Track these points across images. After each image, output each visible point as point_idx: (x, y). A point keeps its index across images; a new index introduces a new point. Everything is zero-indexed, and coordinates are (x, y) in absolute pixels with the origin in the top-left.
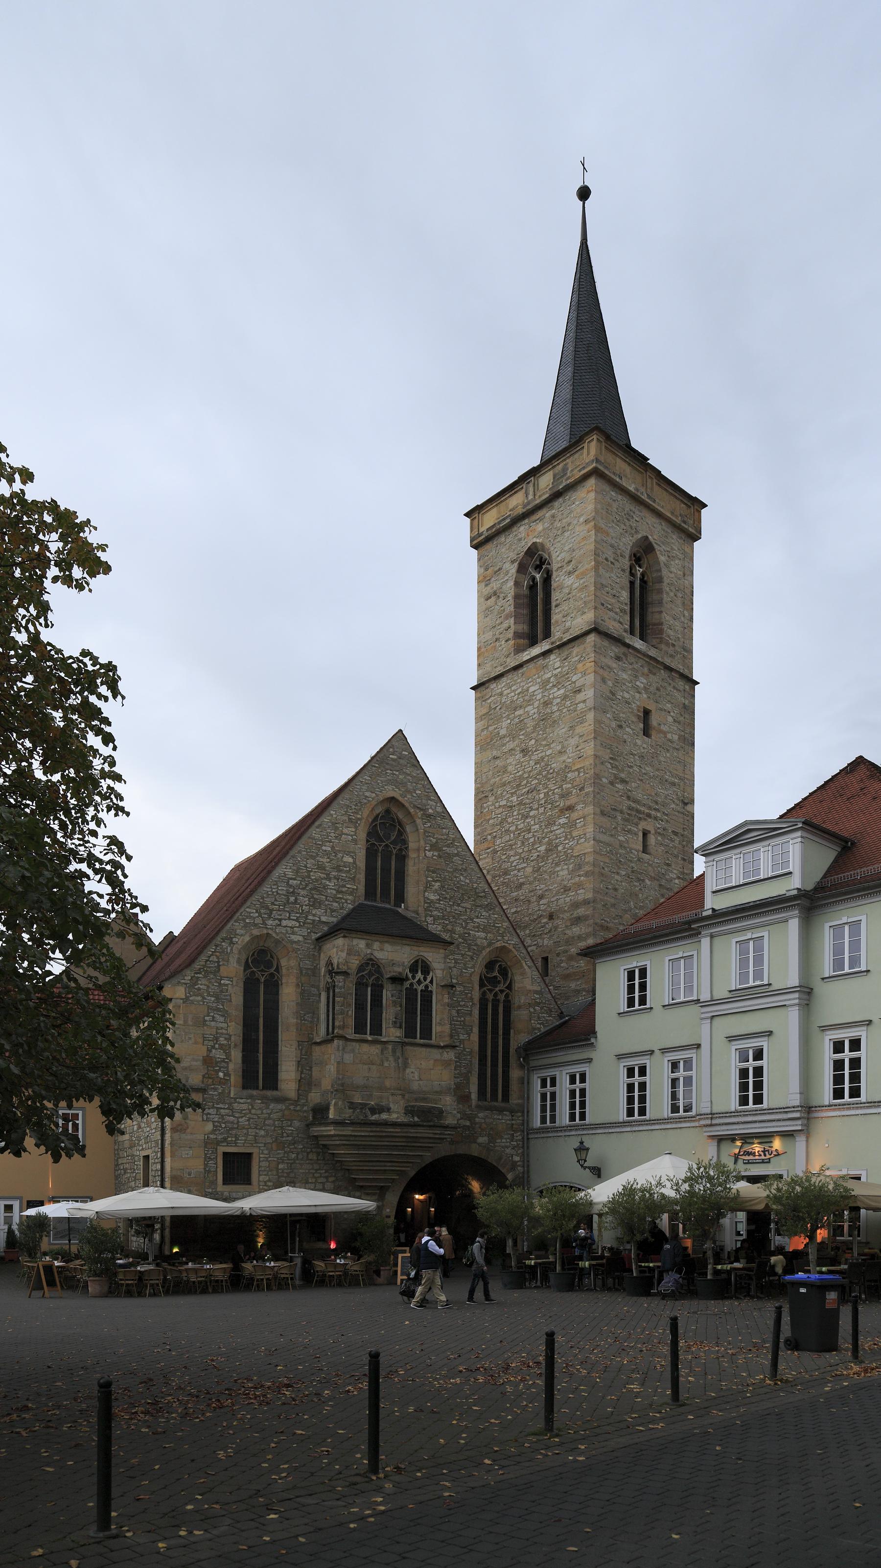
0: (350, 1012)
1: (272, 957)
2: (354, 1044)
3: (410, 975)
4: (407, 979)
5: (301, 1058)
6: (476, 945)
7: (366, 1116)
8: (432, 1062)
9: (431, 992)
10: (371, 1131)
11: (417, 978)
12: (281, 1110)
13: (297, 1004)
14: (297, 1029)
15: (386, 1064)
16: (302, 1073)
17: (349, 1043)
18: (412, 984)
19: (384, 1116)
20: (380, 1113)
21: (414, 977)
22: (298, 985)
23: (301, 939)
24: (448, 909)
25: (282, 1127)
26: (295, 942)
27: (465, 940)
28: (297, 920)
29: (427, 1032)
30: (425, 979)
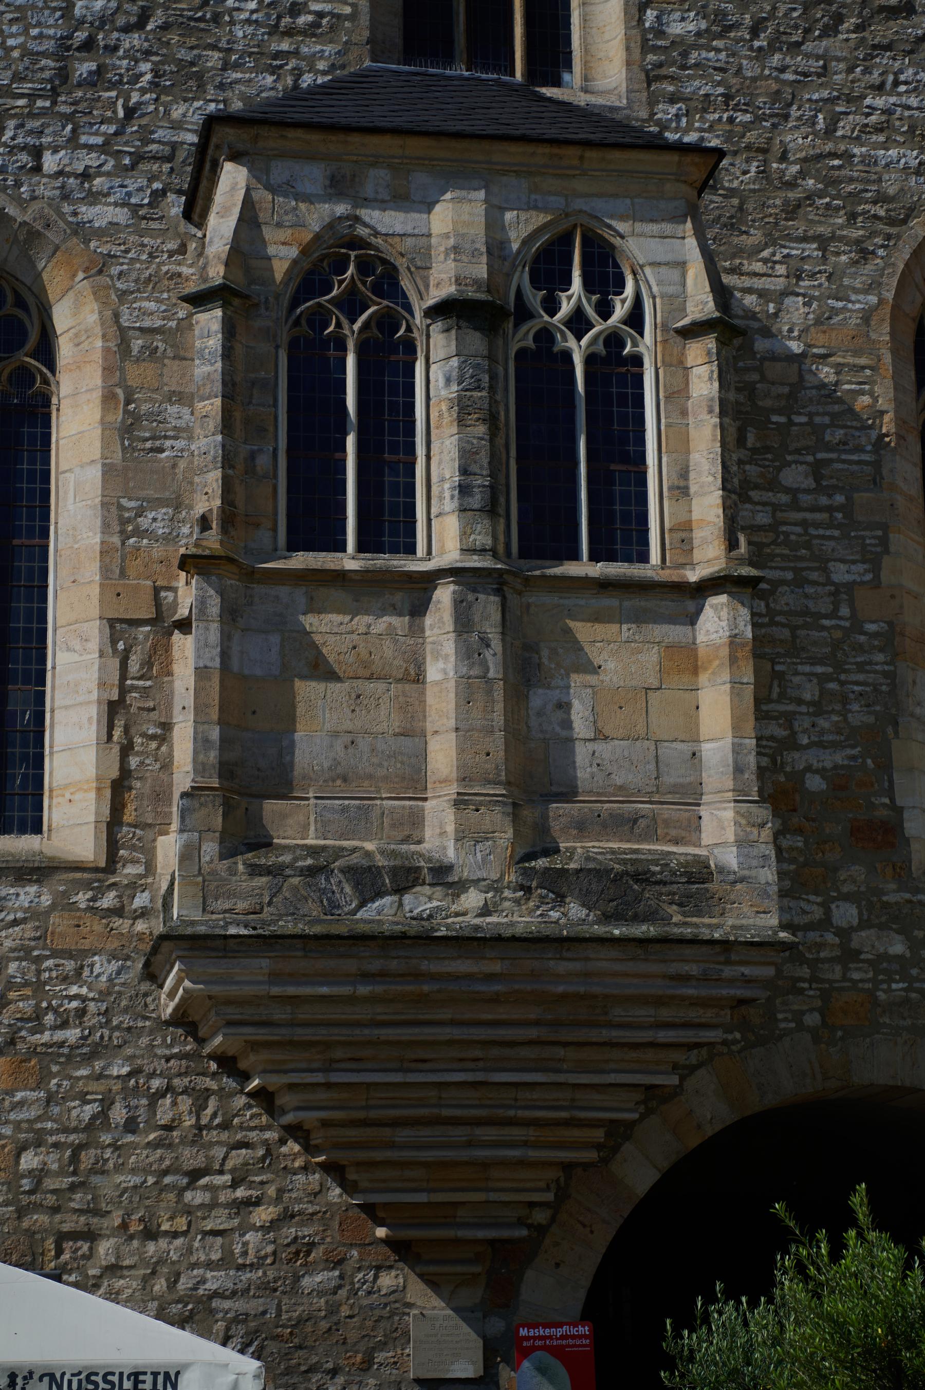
0: (263, 461)
1: (21, 303)
2: (283, 591)
3: (535, 298)
4: (523, 313)
5: (123, 691)
6: (881, 198)
7: (334, 905)
8: (651, 657)
9: (637, 360)
10: (366, 977)
11: (566, 308)
12: (34, 914)
13: (108, 471)
14: (105, 571)
15: (434, 672)
16: (126, 750)
17: (259, 589)
18: (545, 336)
19: (422, 902)
20: (400, 890)
21: (552, 307)
22: (108, 398)
23: (121, 216)
24: (750, 69)
25: (38, 986)
26: (100, 233)
27: (835, 182)
28: (104, 148)
29: (621, 530)
30: (605, 311)
